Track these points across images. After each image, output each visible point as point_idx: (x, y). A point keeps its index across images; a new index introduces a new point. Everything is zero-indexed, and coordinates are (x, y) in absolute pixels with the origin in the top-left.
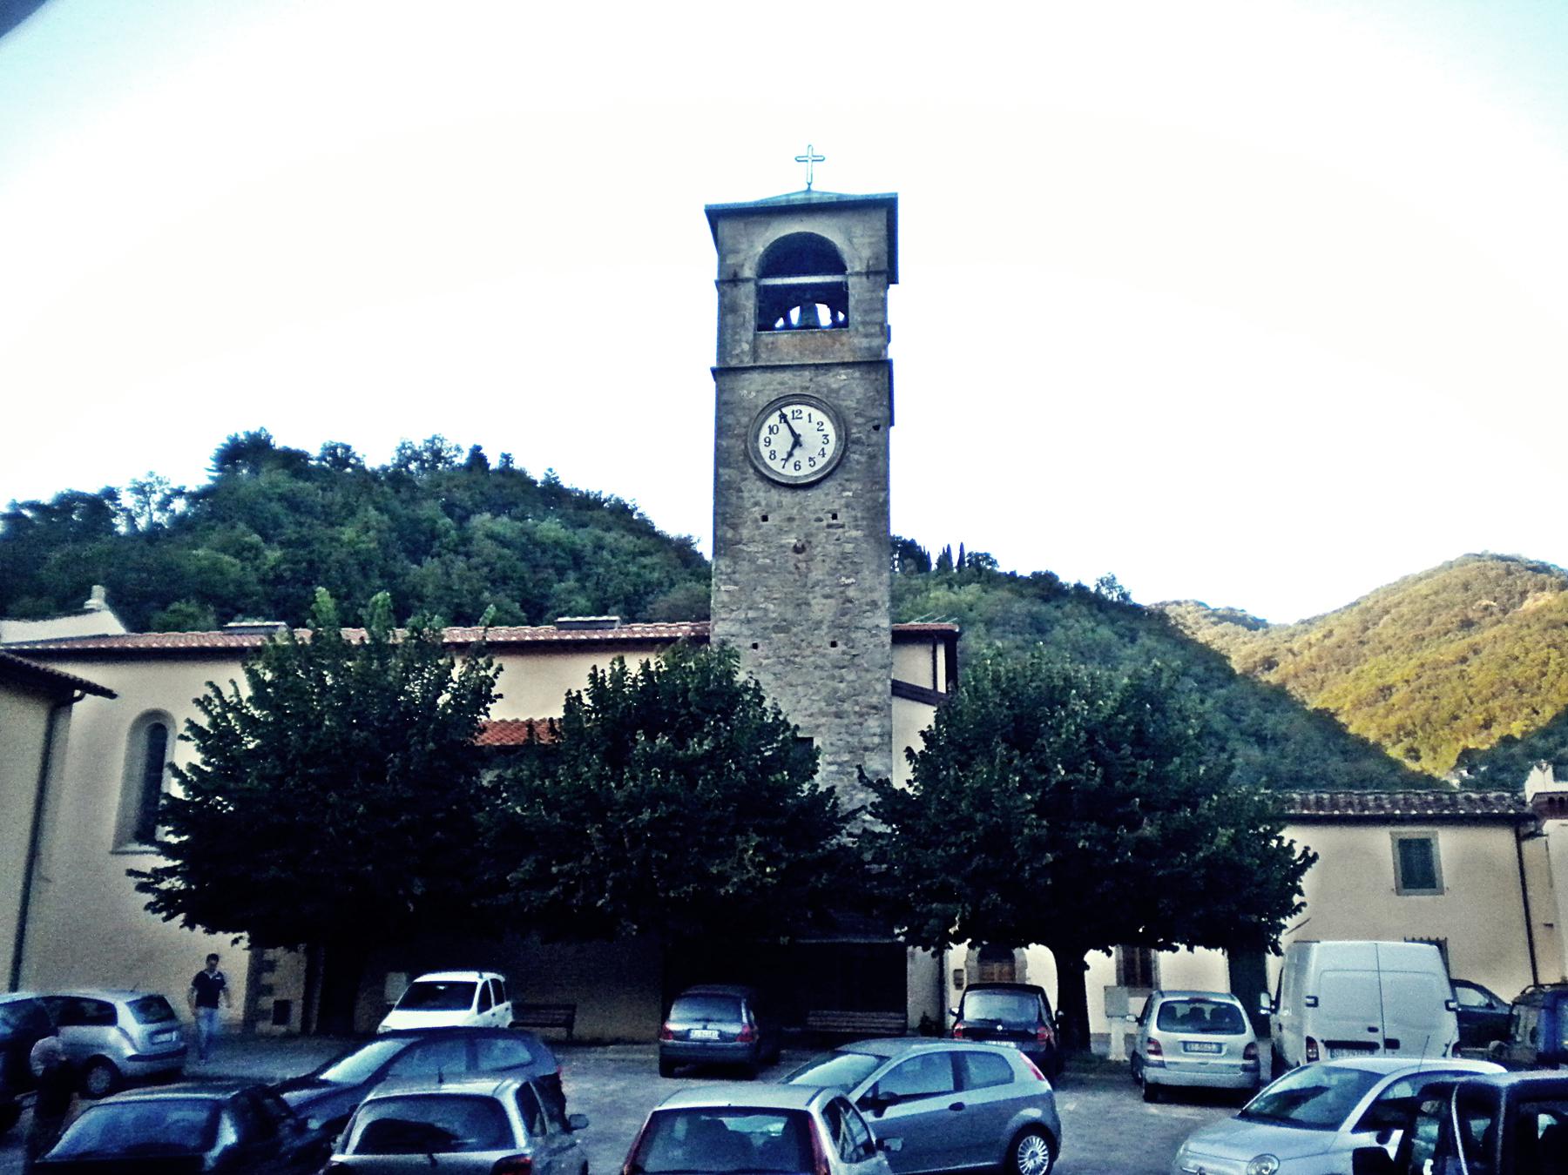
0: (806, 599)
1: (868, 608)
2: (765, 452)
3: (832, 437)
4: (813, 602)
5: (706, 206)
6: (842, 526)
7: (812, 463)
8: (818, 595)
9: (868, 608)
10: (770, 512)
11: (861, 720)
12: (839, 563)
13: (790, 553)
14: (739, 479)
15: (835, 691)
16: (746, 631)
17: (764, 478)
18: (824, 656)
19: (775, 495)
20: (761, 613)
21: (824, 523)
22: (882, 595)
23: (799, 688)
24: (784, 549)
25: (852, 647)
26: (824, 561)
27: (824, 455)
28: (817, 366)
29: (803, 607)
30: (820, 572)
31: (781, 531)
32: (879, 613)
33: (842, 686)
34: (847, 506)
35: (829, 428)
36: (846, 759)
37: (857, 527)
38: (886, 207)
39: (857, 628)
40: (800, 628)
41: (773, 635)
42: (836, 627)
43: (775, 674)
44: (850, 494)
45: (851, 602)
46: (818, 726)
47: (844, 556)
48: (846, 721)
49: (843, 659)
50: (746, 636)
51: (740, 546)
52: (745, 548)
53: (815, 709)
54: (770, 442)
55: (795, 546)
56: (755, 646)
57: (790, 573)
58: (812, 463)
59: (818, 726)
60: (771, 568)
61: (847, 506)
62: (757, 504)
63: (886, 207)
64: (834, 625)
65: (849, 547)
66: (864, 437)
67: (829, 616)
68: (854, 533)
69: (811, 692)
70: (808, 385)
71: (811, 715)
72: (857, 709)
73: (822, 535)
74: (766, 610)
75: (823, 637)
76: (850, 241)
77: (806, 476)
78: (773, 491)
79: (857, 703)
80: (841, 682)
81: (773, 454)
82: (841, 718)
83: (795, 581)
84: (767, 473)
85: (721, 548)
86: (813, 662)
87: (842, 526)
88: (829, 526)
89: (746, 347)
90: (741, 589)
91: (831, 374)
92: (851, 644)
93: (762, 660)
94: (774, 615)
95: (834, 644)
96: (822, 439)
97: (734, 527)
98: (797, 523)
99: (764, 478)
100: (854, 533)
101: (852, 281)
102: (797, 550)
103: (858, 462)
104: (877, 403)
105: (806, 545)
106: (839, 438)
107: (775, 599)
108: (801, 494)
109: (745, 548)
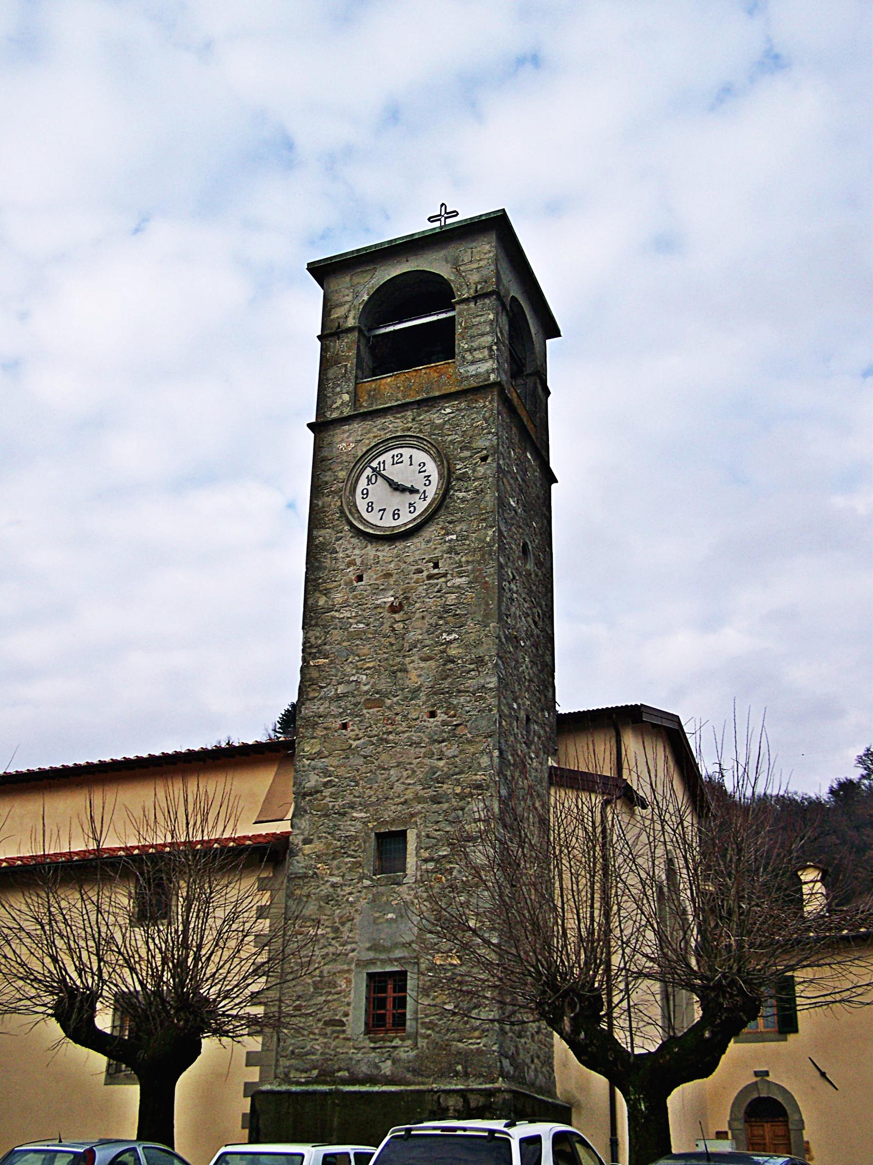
0: (403, 664)
1: (472, 666)
2: (362, 505)
3: (435, 478)
4: (410, 667)
5: (308, 264)
6: (445, 575)
7: (412, 509)
8: (416, 658)
9: (472, 666)
10: (366, 570)
11: (461, 804)
12: (440, 618)
13: (386, 614)
14: (334, 539)
15: (433, 770)
16: (335, 710)
17: (359, 533)
18: (420, 730)
19: (371, 551)
20: (352, 686)
21: (425, 573)
22: (489, 649)
23: (392, 772)
24: (379, 610)
25: (454, 716)
26: (423, 618)
28: (419, 403)
29: (399, 674)
30: (419, 632)
31: (377, 590)
32: (484, 670)
33: (441, 763)
35: (432, 468)
36: (445, 853)
37: (460, 575)
39: (459, 691)
40: (395, 699)
41: (365, 711)
42: (435, 693)
44: (454, 537)
45: (453, 662)
46: (412, 815)
48: (445, 806)
49: (443, 731)
50: (334, 716)
51: (333, 613)
52: (337, 614)
53: (409, 795)
54: (367, 494)
57: (386, 636)
58: (412, 509)
59: (412, 815)
60: (365, 632)
62: (352, 563)
64: (434, 692)
66: (470, 472)
68: (458, 581)
69: (405, 774)
70: (410, 425)
71: (405, 803)
72: (458, 790)
73: (421, 589)
75: (418, 710)
77: (405, 524)
78: (369, 547)
79: (458, 783)
80: (441, 759)
81: (370, 506)
82: (440, 803)
83: (392, 645)
84: (361, 527)
85: (312, 618)
86: (409, 738)
87: (445, 575)
88: (430, 577)
89: (346, 397)
90: (331, 662)
91: (435, 410)
92: (453, 712)
93: (351, 742)
94: (366, 688)
95: (433, 715)
96: (424, 481)
97: (327, 593)
99: (359, 533)
100: (458, 581)
102: (393, 609)
103: (463, 500)
104: (485, 431)
106: (441, 475)
107: (368, 668)
108: (400, 545)
109: (337, 614)
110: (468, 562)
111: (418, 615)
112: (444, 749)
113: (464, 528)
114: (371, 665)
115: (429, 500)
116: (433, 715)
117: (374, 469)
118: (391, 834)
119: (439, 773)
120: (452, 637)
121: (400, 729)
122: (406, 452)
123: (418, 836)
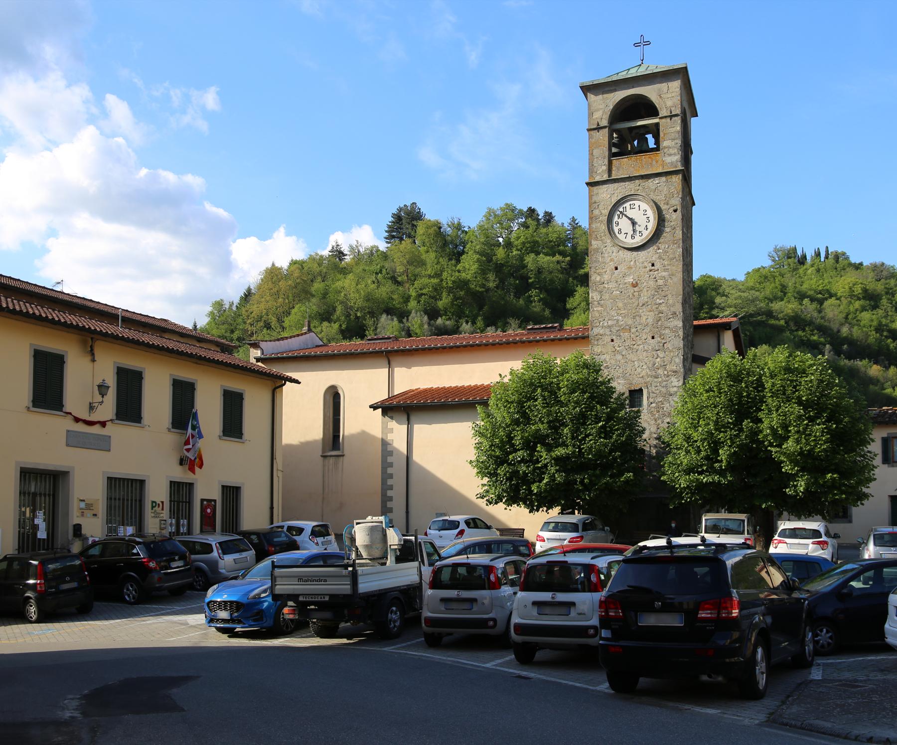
3: (652, 219)
4: (642, 314)
7: (641, 234)
8: (645, 310)
21: (648, 269)
27: (647, 229)
34: (660, 258)
37: (665, 270)
38: (682, 74)
42: (654, 327)
43: (623, 355)
44: (661, 251)
47: (659, 287)
53: (643, 373)
55: (632, 283)
56: (612, 341)
61: (660, 258)
63: (682, 74)
65: (660, 282)
67: (650, 321)
68: (664, 274)
70: (638, 188)
71: (642, 377)
74: (618, 321)
75: (646, 335)
76: (661, 97)
88: (651, 271)
94: (622, 323)
95: (653, 338)
96: (646, 220)
98: (634, 269)
100: (664, 274)
101: (662, 122)
102: (635, 285)
105: (638, 282)
110: (668, 265)
111: (645, 290)
112: (659, 354)
113: (667, 247)
114: (624, 312)
115: (649, 230)
116: (653, 338)
117: (621, 212)
118: (635, 391)
119: (657, 364)
120: (661, 301)
121: (639, 343)
122: (637, 203)
123: (649, 393)
